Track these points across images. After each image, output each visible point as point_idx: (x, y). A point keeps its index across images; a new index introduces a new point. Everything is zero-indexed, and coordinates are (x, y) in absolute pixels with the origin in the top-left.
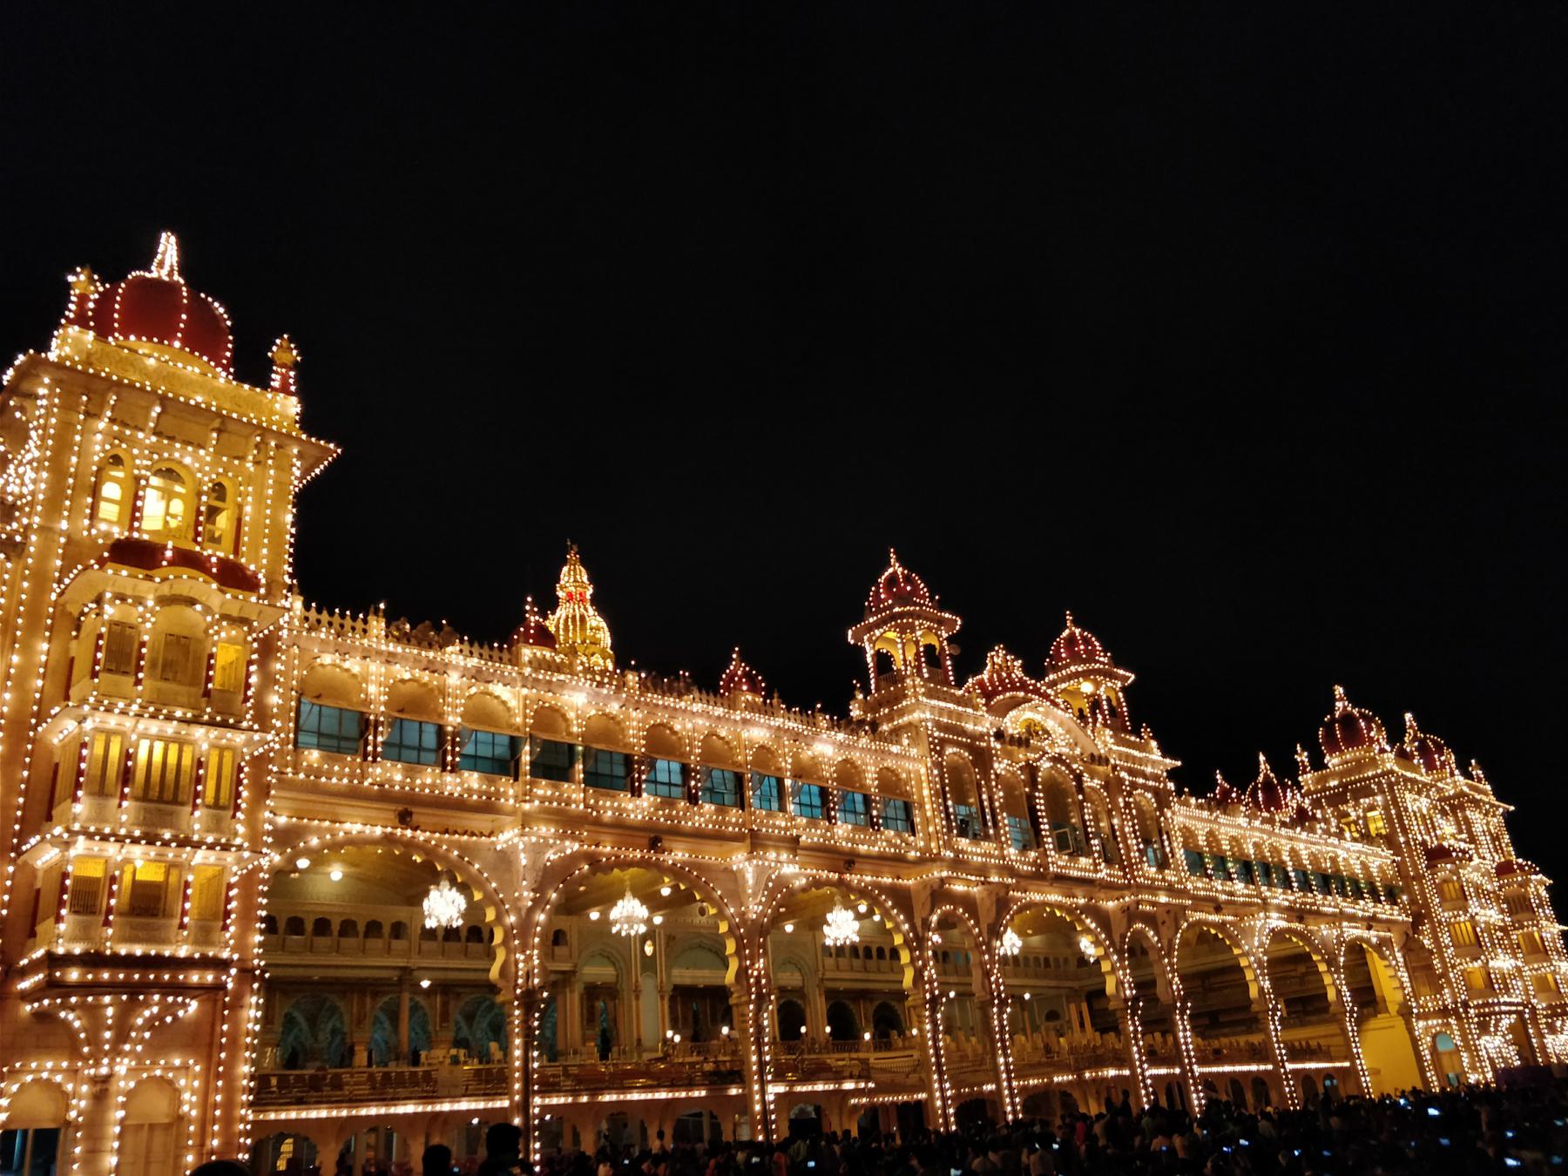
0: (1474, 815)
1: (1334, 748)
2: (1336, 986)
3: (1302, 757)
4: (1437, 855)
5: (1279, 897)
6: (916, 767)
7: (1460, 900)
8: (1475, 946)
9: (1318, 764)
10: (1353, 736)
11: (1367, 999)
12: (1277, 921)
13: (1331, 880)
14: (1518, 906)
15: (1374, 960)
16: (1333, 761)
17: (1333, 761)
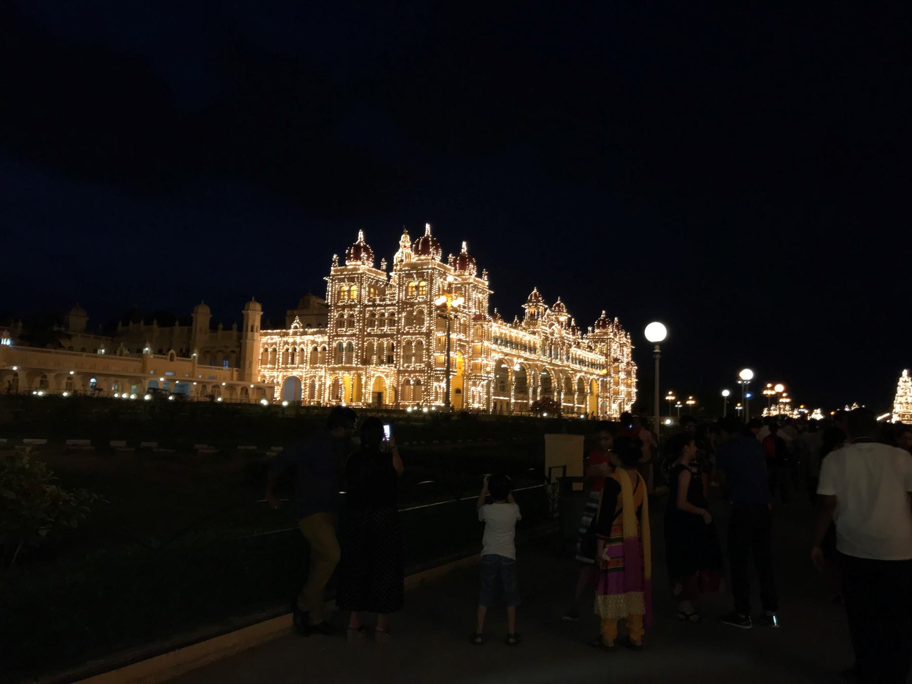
0: (625, 349)
1: (598, 328)
2: (587, 389)
3: (590, 329)
4: (616, 360)
5: (585, 369)
6: (537, 340)
7: (617, 372)
8: (617, 384)
9: (593, 331)
10: (604, 326)
11: (591, 393)
12: (583, 374)
13: (593, 365)
14: (628, 374)
15: (595, 384)
16: (597, 331)
17: (597, 331)
